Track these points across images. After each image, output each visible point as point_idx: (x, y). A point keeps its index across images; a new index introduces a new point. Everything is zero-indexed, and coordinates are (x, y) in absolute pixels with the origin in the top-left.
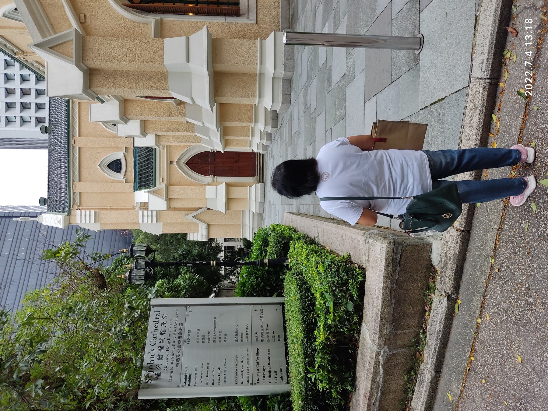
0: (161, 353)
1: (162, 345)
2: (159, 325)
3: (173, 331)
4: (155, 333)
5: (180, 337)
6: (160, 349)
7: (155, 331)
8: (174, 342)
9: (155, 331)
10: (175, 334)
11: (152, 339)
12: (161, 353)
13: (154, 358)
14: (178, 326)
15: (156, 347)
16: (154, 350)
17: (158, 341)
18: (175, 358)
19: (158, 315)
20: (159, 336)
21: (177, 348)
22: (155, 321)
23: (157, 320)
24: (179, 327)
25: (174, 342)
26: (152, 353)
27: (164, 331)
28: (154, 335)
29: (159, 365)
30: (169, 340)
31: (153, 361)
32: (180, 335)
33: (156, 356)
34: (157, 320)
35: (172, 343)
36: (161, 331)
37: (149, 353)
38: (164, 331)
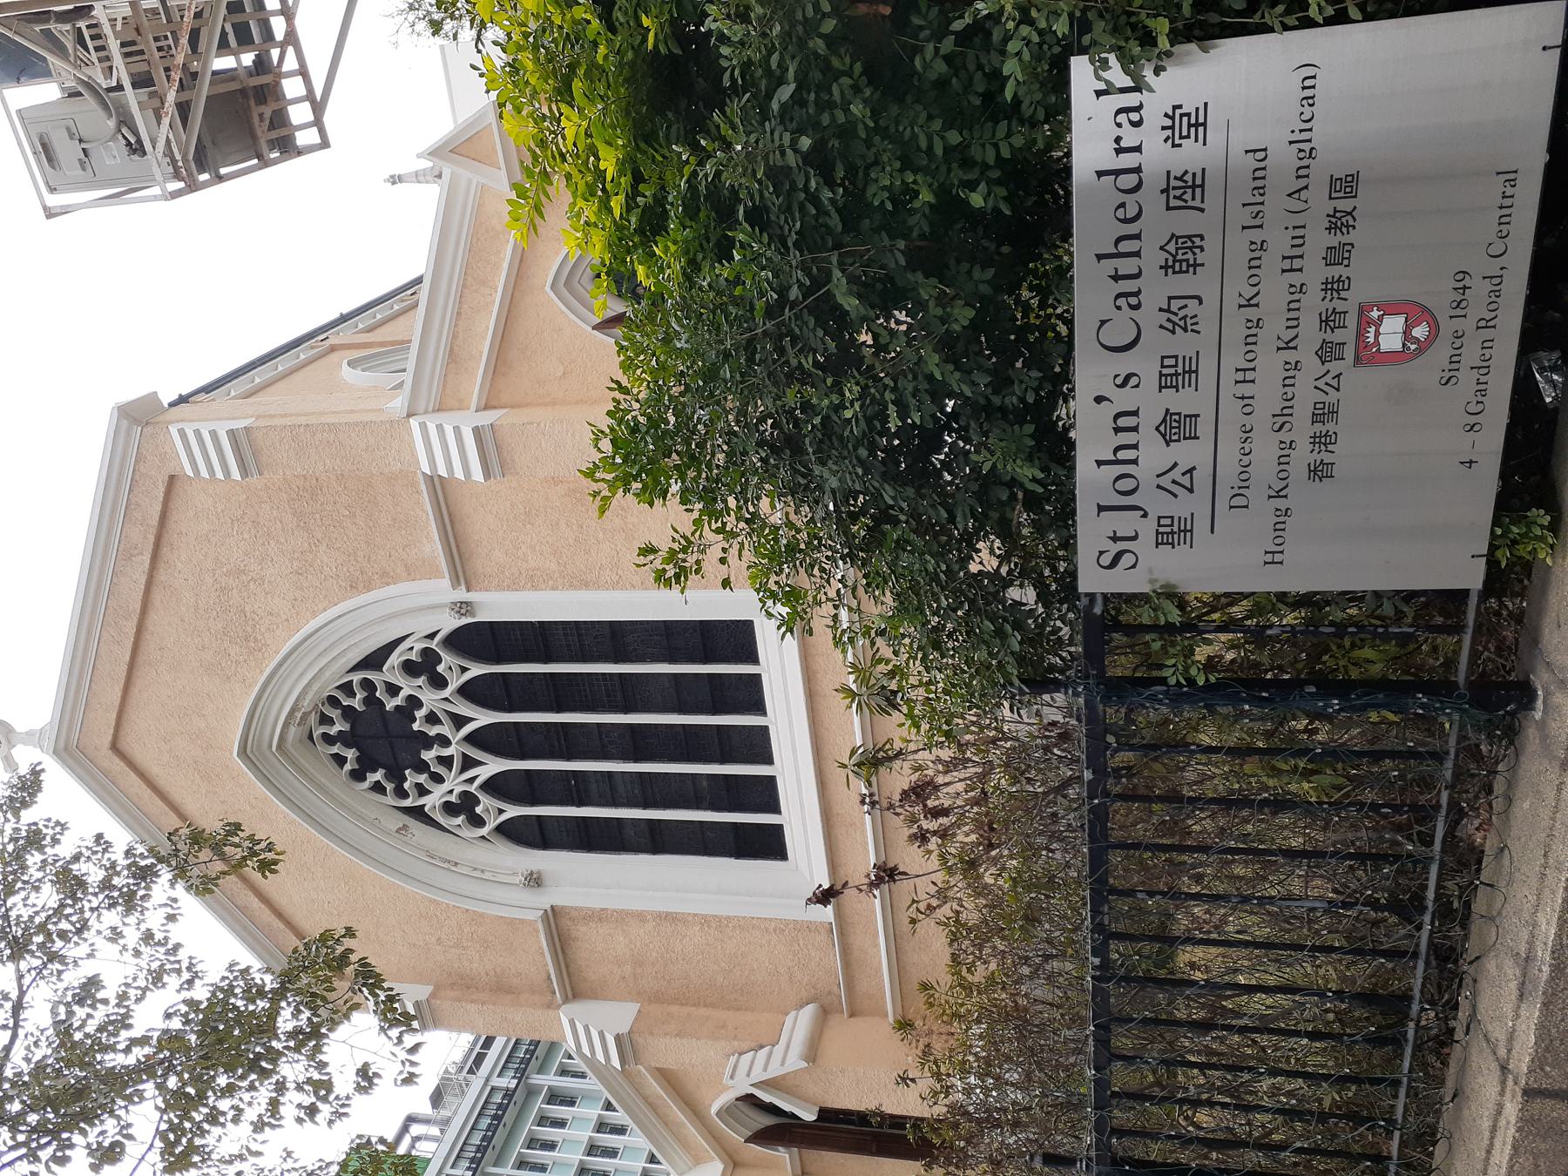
0: (1182, 401)
1: (1182, 344)
2: (1151, 199)
3: (1279, 242)
4: (1127, 265)
5: (1334, 287)
6: (1176, 374)
7: (1125, 247)
8: (1294, 323)
9: (1125, 247)
10: (1297, 264)
11: (1110, 312)
12: (1182, 401)
14: (1320, 203)
15: (1145, 363)
16: (1134, 381)
17: (1150, 316)
18: (1302, 429)
20: (1156, 288)
21: (1311, 366)
22: (1117, 173)
23: (1128, 160)
24: (1329, 207)
25: (1294, 323)
26: (1124, 399)
27: (1192, 242)
28: (1116, 278)
29: (1176, 474)
30: (1252, 313)
31: (1135, 447)
32: (1336, 271)
33: (1150, 418)
35: (1274, 327)
36: (1171, 247)
37: (1099, 399)
38: (1192, 242)
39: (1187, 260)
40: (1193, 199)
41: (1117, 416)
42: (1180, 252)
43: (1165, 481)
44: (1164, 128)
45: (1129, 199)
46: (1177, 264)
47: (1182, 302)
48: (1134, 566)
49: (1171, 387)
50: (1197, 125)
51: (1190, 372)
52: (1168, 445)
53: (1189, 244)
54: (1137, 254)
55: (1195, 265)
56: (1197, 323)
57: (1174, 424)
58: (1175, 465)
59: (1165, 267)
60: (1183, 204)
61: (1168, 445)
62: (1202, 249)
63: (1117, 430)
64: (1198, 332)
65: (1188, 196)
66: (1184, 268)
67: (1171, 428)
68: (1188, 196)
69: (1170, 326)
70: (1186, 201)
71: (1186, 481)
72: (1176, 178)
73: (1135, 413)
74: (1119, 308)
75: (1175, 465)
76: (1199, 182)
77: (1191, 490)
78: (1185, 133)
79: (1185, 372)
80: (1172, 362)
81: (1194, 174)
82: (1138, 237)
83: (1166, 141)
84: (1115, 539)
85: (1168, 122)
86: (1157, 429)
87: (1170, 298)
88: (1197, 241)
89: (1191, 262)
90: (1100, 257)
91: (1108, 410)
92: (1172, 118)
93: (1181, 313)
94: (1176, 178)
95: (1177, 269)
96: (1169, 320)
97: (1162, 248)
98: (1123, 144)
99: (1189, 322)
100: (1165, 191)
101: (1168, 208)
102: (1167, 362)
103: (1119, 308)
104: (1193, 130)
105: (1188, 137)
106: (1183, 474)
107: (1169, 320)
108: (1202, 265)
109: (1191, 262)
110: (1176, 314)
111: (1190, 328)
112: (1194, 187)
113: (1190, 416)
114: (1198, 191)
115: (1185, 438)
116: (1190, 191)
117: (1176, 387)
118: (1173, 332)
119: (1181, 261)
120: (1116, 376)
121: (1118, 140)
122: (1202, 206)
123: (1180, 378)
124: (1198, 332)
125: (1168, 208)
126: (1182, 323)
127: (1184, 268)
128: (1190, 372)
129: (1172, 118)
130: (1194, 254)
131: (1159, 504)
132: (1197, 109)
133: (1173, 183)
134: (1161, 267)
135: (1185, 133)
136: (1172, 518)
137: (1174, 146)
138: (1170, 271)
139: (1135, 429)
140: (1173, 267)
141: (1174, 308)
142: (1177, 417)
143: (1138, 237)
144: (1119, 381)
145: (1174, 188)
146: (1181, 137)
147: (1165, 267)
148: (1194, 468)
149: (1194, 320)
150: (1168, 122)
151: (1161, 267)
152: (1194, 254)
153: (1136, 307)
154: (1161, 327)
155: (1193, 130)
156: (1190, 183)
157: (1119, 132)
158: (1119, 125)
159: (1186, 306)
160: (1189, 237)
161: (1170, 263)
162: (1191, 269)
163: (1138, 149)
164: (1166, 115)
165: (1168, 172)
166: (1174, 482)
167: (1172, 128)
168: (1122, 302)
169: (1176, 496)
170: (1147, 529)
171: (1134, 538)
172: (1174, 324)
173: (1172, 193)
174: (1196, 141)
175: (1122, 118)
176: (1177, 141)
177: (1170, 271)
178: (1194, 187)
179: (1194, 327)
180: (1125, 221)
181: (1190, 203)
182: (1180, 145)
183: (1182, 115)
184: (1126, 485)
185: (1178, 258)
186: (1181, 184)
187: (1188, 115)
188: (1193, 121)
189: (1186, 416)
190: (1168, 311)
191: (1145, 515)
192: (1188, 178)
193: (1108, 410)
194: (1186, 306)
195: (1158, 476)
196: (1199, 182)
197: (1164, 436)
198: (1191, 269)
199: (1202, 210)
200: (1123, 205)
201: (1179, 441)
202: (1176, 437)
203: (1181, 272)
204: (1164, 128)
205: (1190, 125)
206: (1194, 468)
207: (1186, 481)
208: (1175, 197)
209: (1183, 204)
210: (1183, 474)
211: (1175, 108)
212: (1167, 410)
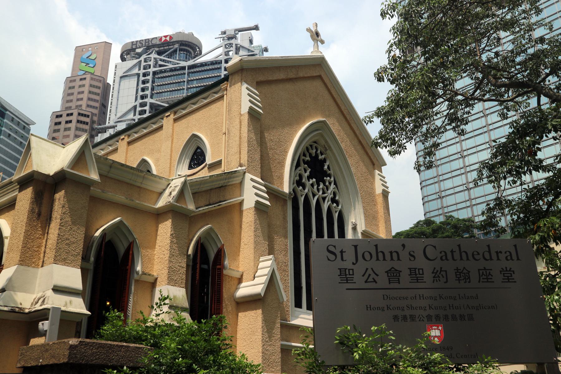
0: (405, 277)
4: (457, 255)
7: (464, 255)
9: (464, 255)
12: (405, 277)
13: (392, 259)
15: (421, 262)
16: (412, 258)
19: (509, 258)
22: (489, 252)
23: (494, 256)
26: (404, 255)
27: (467, 278)
28: (452, 252)
31: (384, 259)
33: (396, 265)
34: (494, 256)
36: (465, 271)
39: (461, 277)
40: (483, 279)
41: (397, 252)
42: (464, 274)
43: (369, 271)
44: (506, 268)
45: (481, 256)
46: (459, 273)
47: (445, 275)
48: (329, 260)
49: (411, 273)
50: (508, 279)
51: (417, 280)
52: (386, 272)
53: (467, 278)
54: (461, 259)
55: (459, 280)
56: (437, 281)
57: (395, 274)
58: (377, 275)
59: (457, 269)
60: (481, 275)
61: (386, 272)
62: (465, 282)
63: (391, 253)
64: (433, 282)
65: (484, 277)
66: (458, 276)
67: (393, 273)
68: (484, 277)
69: (435, 271)
70: (482, 276)
71: (370, 279)
72: (490, 272)
73: (399, 259)
74: (441, 253)
75: (377, 275)
76: (489, 280)
77: (366, 282)
78: (505, 275)
79: (417, 277)
80: (421, 272)
81: (491, 279)
82: (468, 259)
83: (502, 269)
84: (342, 252)
85: (508, 269)
86: (393, 268)
87: (446, 271)
88: (468, 280)
89: (460, 279)
90: (459, 246)
91: (400, 249)
92: (510, 271)
93: (440, 275)
94: (490, 272)
95: (457, 273)
96: (437, 271)
97: (464, 268)
98: (500, 254)
99: (437, 278)
100: (485, 269)
101: (479, 270)
102: (421, 271)
103: (441, 253)
104: (507, 278)
105: (504, 276)
106: (373, 279)
107: (437, 271)
108: (459, 283)
109: (460, 279)
110: (440, 274)
111: (435, 279)
112: (487, 279)
113: (399, 280)
114: (486, 280)
115: (389, 279)
116: (486, 277)
117: (411, 275)
118: (433, 273)
119: (460, 275)
120: (414, 252)
121: (501, 252)
122: (481, 282)
123: (415, 276)
124: (433, 282)
125: (479, 270)
126: (437, 276)
127: (458, 276)
128: (417, 280)
129: (510, 271)
130: (463, 279)
131: (359, 269)
132: (513, 279)
133: (488, 272)
134: (457, 268)
135: (505, 275)
136: (353, 275)
137: (501, 271)
138: (456, 271)
139: (392, 259)
140: (458, 272)
141: (442, 273)
142: (398, 275)
143: (468, 259)
144: (412, 253)
145: (486, 272)
146: (504, 274)
147: (457, 269)
148: (376, 283)
149: (438, 280)
150: (508, 269)
151: (457, 268)
152: (463, 279)
153: (441, 258)
154: (435, 268)
155: (507, 278)
156: (488, 277)
157: (503, 253)
158: (506, 253)
159: (443, 277)
160: (469, 278)
161: (459, 271)
162: (457, 279)
163: (498, 259)
164: (511, 269)
165: (491, 270)
166: (370, 275)
167: (507, 271)
168: (443, 254)
169: (363, 276)
170: (347, 264)
171: (342, 259)
172: (436, 273)
173: (484, 271)
174: (503, 279)
175: (508, 254)
176: (502, 272)
177: (456, 271)
178: (487, 279)
179: (435, 281)
180: (473, 255)
181: (481, 278)
182: (501, 273)
183: (511, 274)
184: (367, 256)
185: (462, 274)
186: (488, 274)
187: (511, 276)
188: (510, 278)
189: (399, 279)
190: (441, 271)
191: (353, 264)
192: (490, 277)
193: (400, 249)
194: (443, 277)
195: (372, 269)
196: (489, 280)
197: (390, 270)
198: (457, 279)
199: (479, 282)
200: (478, 254)
201: (388, 276)
202: (389, 275)
203: (456, 275)
204: (506, 268)
205: (508, 277)
206: (376, 283)
207: (370, 279)
208: (483, 272)
209: (481, 275)
210: (373, 279)
211: (513, 271)
212: (401, 271)
